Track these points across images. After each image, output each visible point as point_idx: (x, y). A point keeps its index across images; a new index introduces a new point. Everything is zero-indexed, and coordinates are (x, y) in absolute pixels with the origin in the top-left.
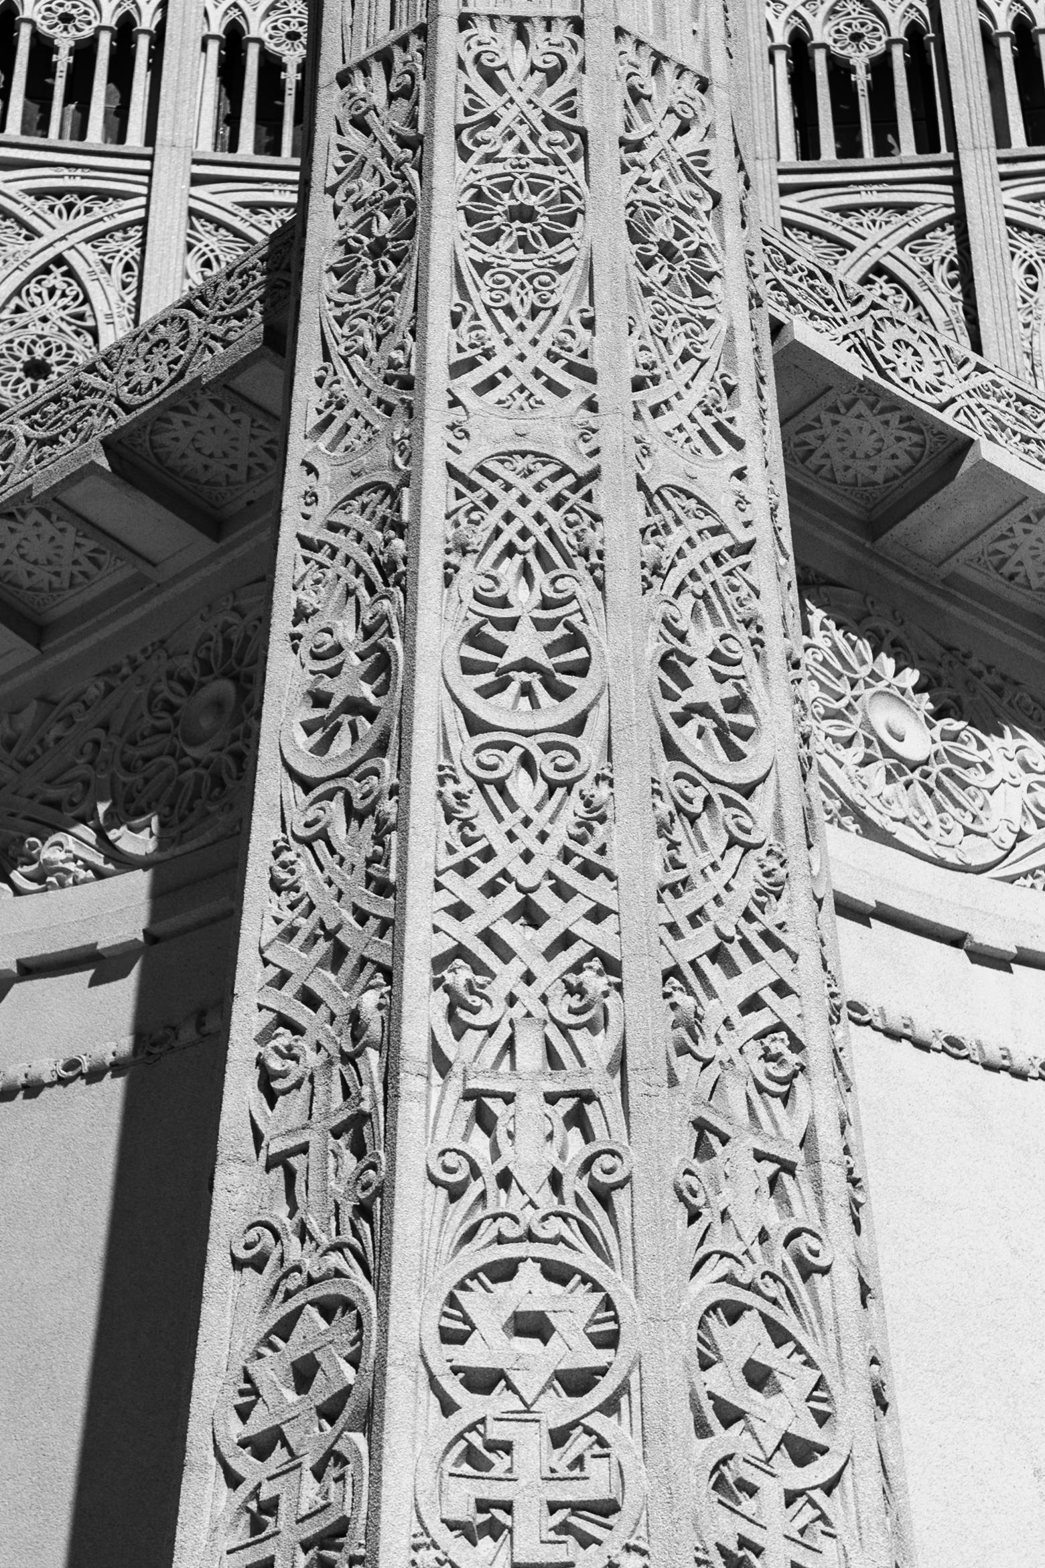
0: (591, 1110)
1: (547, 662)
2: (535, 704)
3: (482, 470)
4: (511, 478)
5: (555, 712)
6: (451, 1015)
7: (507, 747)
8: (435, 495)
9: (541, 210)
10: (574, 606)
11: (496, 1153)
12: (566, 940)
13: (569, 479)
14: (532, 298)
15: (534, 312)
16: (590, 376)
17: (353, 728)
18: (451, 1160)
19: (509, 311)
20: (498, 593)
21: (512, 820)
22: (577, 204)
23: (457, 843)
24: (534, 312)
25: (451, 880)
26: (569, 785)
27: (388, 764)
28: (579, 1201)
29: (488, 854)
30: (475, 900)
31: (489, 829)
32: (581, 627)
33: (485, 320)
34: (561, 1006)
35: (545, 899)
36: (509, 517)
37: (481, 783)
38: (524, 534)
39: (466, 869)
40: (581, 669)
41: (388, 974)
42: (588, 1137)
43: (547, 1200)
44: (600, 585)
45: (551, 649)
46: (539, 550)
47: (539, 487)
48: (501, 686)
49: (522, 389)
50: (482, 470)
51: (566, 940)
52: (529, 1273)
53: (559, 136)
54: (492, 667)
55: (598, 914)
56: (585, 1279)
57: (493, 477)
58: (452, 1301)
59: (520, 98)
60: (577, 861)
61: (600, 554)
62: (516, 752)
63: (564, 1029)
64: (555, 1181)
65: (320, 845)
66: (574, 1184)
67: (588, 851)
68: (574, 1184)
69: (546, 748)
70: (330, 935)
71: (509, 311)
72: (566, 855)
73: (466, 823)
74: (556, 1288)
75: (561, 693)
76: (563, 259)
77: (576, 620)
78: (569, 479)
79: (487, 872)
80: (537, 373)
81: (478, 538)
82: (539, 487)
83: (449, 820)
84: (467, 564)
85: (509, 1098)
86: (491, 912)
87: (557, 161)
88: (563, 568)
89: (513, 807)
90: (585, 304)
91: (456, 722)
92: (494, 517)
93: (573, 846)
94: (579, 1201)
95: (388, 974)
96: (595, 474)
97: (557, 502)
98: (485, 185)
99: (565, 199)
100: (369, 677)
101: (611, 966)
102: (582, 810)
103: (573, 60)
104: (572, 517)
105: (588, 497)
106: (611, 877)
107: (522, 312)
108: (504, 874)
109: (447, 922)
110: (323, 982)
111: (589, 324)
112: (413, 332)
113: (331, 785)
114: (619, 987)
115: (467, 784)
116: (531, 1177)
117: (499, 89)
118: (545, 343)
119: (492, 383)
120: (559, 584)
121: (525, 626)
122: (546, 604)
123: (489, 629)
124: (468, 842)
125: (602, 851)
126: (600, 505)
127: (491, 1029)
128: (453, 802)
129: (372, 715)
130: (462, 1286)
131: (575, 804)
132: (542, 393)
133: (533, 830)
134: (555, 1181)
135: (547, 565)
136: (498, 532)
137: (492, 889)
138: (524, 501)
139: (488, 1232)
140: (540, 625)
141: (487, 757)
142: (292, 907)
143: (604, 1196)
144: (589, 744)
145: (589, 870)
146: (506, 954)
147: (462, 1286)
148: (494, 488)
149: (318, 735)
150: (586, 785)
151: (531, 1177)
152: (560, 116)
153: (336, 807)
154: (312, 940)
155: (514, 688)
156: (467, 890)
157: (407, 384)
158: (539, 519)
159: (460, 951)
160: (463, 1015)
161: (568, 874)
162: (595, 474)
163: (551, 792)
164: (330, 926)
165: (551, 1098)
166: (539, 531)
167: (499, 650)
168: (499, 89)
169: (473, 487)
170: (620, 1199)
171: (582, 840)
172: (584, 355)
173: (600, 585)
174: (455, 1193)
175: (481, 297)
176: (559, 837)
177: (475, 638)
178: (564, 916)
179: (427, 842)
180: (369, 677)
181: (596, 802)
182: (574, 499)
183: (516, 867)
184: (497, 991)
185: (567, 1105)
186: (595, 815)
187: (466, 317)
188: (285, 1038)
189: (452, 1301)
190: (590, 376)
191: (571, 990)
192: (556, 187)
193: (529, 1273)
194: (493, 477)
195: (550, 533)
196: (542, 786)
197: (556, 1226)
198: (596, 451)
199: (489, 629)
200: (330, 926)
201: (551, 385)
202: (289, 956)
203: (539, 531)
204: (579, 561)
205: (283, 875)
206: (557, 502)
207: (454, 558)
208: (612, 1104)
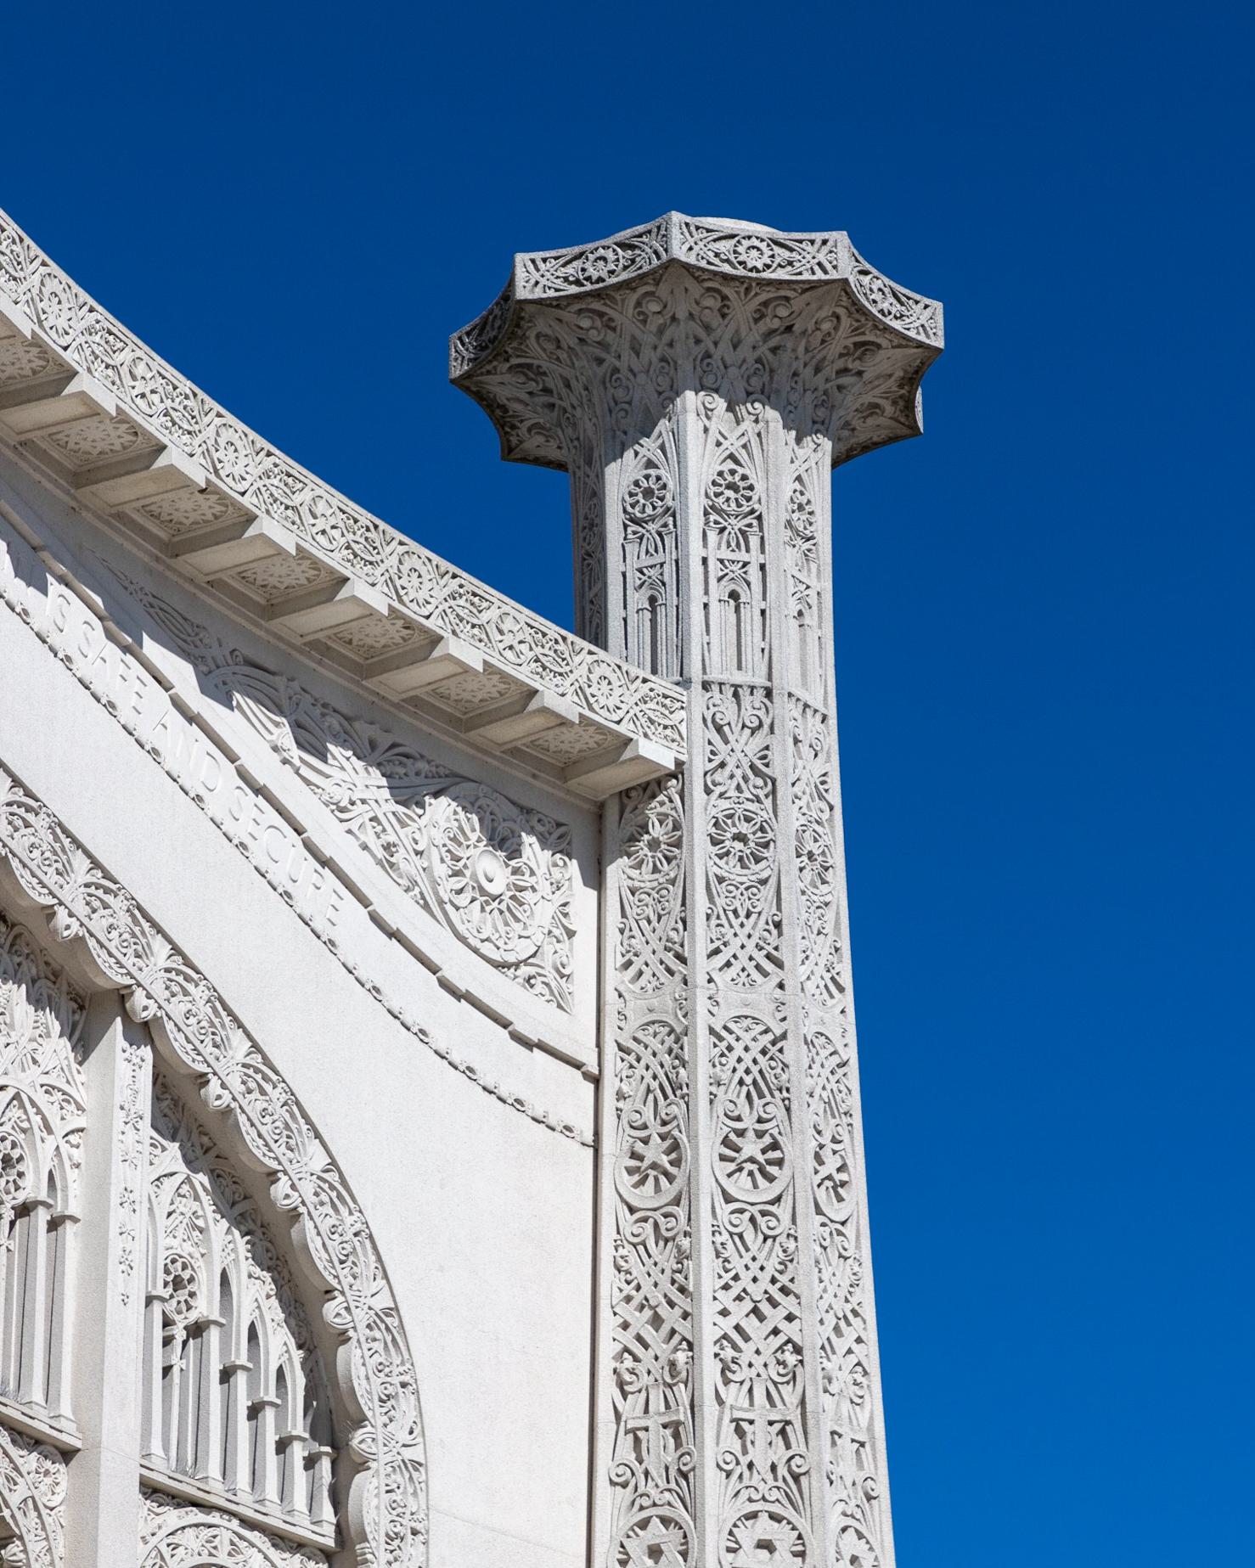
0: (789, 1429)
1: (761, 1158)
2: (755, 1186)
3: (725, 1028)
4: (740, 1033)
5: (768, 1191)
6: (723, 1372)
7: (741, 1211)
8: (702, 1047)
9: (751, 837)
10: (774, 1123)
11: (745, 1452)
12: (776, 1332)
13: (770, 1037)
14: (748, 904)
15: (748, 916)
16: (779, 964)
17: (656, 1179)
18: (729, 1458)
19: (735, 912)
20: (736, 1113)
21: (747, 1257)
22: (770, 835)
23: (722, 1273)
24: (748, 916)
25: (720, 1294)
26: (774, 1238)
27: (681, 1211)
28: (784, 1480)
29: (736, 1278)
30: (732, 1306)
31: (737, 1264)
32: (779, 1137)
33: (724, 921)
34: (773, 1371)
35: (765, 1307)
36: (739, 1060)
37: (731, 1234)
38: (748, 1071)
39: (726, 1287)
40: (779, 1163)
41: (691, 1347)
42: (788, 1447)
43: (769, 1477)
44: (788, 1109)
45: (764, 1151)
46: (755, 1082)
47: (754, 1039)
48: (740, 1169)
49: (743, 970)
50: (725, 1028)
51: (776, 1332)
52: (764, 1517)
53: (760, 782)
54: (732, 1160)
55: (790, 1318)
56: (789, 1523)
57: (730, 1032)
58: (731, 1533)
59: (738, 748)
60: (778, 1285)
61: (788, 1090)
62: (747, 1215)
63: (775, 1383)
64: (773, 1468)
65: (641, 1248)
66: (782, 1471)
67: (784, 1280)
68: (782, 1471)
69: (764, 1214)
70: (651, 1307)
71: (735, 912)
72: (773, 1281)
73: (726, 1260)
74: (776, 1525)
75: (770, 1179)
76: (764, 875)
77: (775, 1132)
78: (770, 1037)
79: (736, 1289)
80: (751, 959)
81: (725, 1076)
82: (754, 1039)
83: (718, 1257)
84: (720, 1092)
85: (751, 1422)
86: (740, 1312)
87: (759, 801)
88: (769, 1098)
89: (747, 1250)
90: (774, 911)
91: (719, 1199)
92: (733, 1057)
93: (777, 1275)
94: (784, 1480)
95: (691, 1347)
96: (784, 1036)
97: (764, 1052)
98: (720, 816)
99: (762, 829)
100: (668, 1152)
101: (798, 1350)
102: (781, 1255)
103: (767, 722)
104: (773, 1064)
105: (781, 1051)
106: (797, 1297)
107: (742, 913)
108: (744, 1290)
109: (720, 1319)
110: (649, 1333)
111: (778, 925)
112: (684, 921)
113: (649, 1213)
114: (801, 1362)
115: (726, 1236)
116: (762, 1466)
117: (726, 742)
118: (755, 940)
119: (728, 964)
120: (768, 1109)
121: (751, 1134)
122: (760, 1121)
123: (732, 1136)
124: (727, 1271)
125: (792, 1280)
126: (788, 1057)
127: (742, 1383)
128: (719, 1247)
129: (671, 1178)
130: (735, 1525)
131: (778, 1249)
132: (756, 975)
133: (757, 1265)
134: (773, 1468)
135: (761, 1096)
136: (734, 1070)
137: (739, 1298)
138: (746, 1049)
139: (744, 1494)
140: (760, 1135)
141: (735, 1218)
142: (628, 1283)
143: (796, 1478)
144: (783, 1211)
145: (785, 1291)
146: (747, 1339)
147: (735, 1525)
148: (730, 1039)
149: (636, 1178)
150: (782, 1239)
151: (762, 1466)
152: (758, 763)
153: (649, 1226)
154: (641, 1308)
155: (745, 1172)
156: (727, 1299)
157: (682, 960)
158: (755, 1061)
159: (725, 1337)
160: (729, 1374)
161: (778, 1296)
162: (784, 1036)
163: (765, 1240)
164: (653, 1303)
165: (771, 1423)
166: (755, 1069)
167: (738, 1150)
168: (726, 742)
169: (721, 1039)
170: (803, 1480)
171: (781, 1272)
172: (776, 949)
173: (788, 1109)
174: (729, 1474)
175: (721, 902)
176: (770, 1271)
177: (726, 1142)
178: (775, 1317)
179: (706, 1274)
180: (668, 1152)
181: (790, 1251)
182: (774, 1050)
183: (751, 1288)
184: (744, 1360)
185: (778, 1427)
186: (788, 1260)
187: (714, 917)
188: (629, 1362)
189: (731, 1533)
190: (779, 964)
191: (779, 1363)
192: (759, 820)
193: (764, 1517)
194: (730, 1032)
195: (761, 1072)
196: (761, 1237)
197: (775, 1494)
198: (784, 1019)
199: (732, 1136)
200: (653, 1303)
201: (758, 967)
202: (628, 1312)
203: (755, 1069)
204: (777, 1093)
205: (622, 1263)
206: (764, 1052)
207: (714, 1089)
208: (798, 1424)
